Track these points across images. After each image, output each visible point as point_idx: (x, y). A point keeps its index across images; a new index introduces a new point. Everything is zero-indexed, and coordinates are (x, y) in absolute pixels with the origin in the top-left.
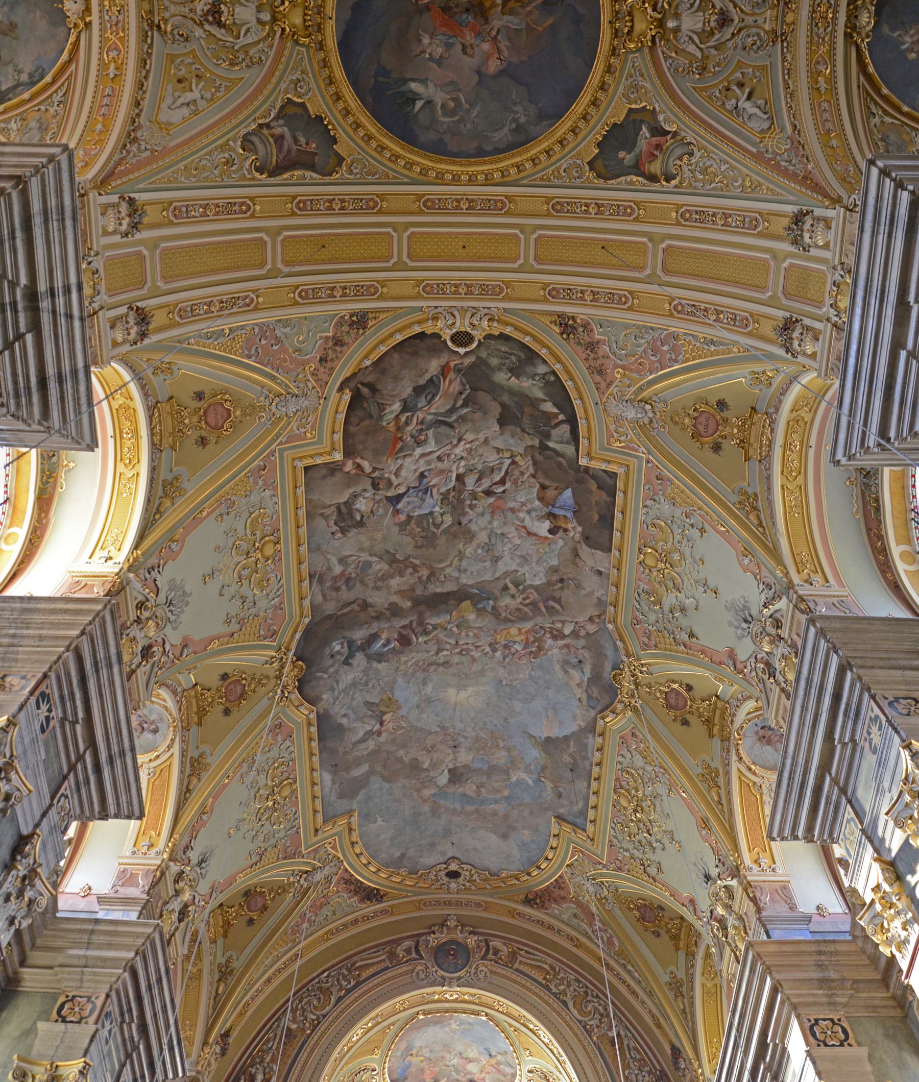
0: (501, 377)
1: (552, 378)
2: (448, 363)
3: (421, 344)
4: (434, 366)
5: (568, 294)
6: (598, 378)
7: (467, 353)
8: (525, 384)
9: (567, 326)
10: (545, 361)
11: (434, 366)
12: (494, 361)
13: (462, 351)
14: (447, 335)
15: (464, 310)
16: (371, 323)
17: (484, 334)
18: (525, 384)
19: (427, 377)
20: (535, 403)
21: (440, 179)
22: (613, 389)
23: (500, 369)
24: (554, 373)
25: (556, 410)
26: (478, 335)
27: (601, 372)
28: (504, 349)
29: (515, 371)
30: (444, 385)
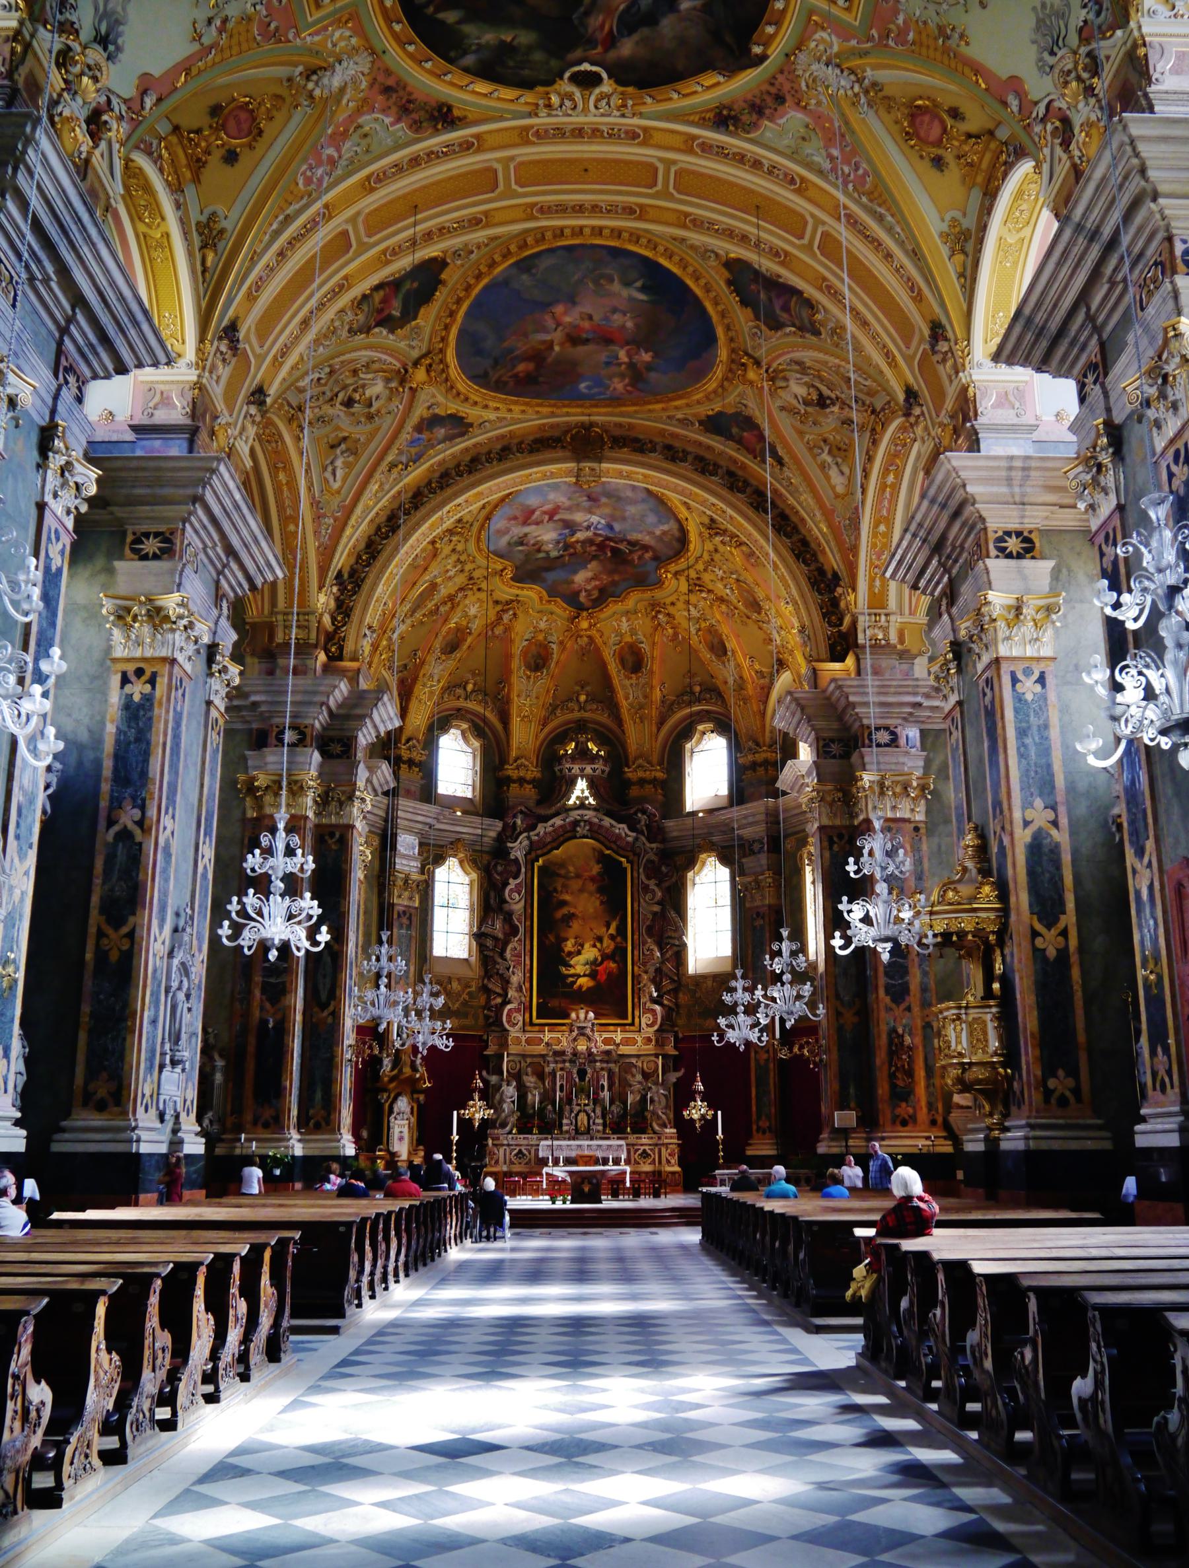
0: (525, 38)
1: (452, 54)
2: (606, 50)
3: (648, 76)
4: (627, 48)
5: (450, 152)
6: (390, 82)
7: (580, 63)
8: (489, 37)
9: (443, 116)
10: (466, 70)
11: (627, 48)
12: (538, 56)
13: (586, 67)
14: (607, 86)
15: (585, 111)
16: (710, 115)
17: (556, 86)
18: (489, 37)
19: (636, 37)
20: (474, 15)
21: (617, 233)
22: (364, 85)
23: (530, 48)
24: (451, 61)
25: (441, 16)
26: (565, 86)
27: (387, 90)
28: (526, 72)
29: (506, 49)
30: (612, 24)
